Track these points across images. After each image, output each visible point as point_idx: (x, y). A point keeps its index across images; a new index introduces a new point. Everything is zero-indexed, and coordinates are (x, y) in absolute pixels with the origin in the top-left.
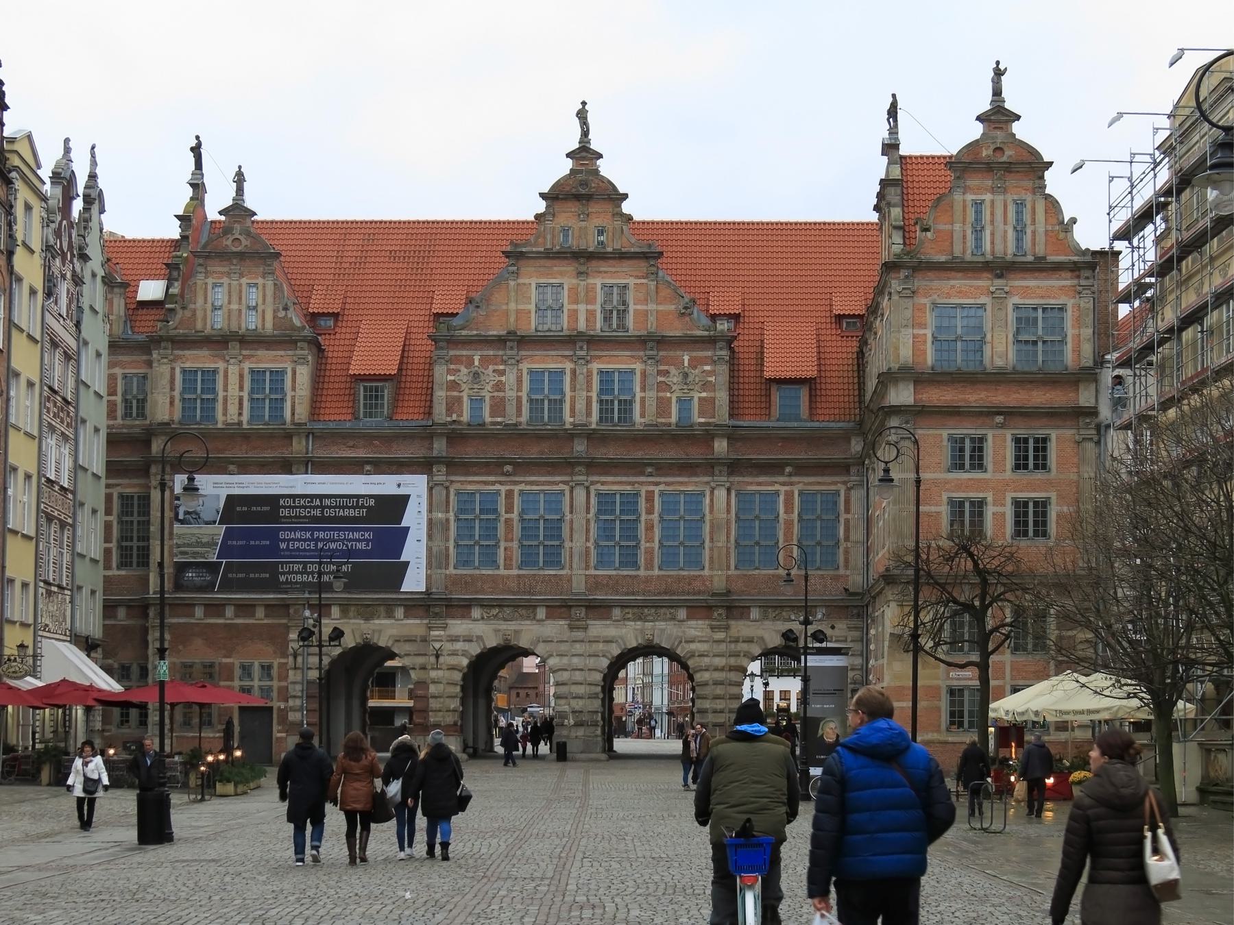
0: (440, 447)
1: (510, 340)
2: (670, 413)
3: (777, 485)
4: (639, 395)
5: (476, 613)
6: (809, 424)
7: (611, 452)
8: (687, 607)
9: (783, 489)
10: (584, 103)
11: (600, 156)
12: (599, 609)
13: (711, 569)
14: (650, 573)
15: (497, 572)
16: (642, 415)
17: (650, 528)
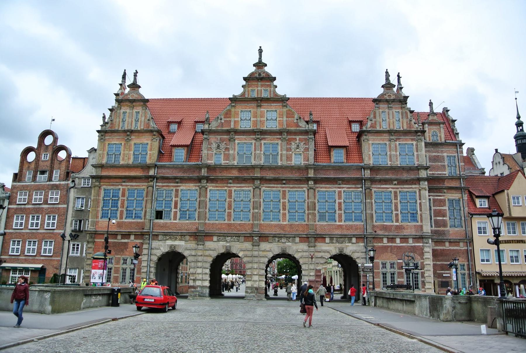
0: (204, 172)
1: (232, 132)
3: (334, 189)
4: (280, 153)
5: (215, 238)
6: (347, 164)
7: (270, 175)
8: (300, 237)
10: (260, 47)
11: (266, 65)
12: (264, 238)
13: (308, 221)
14: (285, 223)
15: (224, 222)
16: (281, 160)
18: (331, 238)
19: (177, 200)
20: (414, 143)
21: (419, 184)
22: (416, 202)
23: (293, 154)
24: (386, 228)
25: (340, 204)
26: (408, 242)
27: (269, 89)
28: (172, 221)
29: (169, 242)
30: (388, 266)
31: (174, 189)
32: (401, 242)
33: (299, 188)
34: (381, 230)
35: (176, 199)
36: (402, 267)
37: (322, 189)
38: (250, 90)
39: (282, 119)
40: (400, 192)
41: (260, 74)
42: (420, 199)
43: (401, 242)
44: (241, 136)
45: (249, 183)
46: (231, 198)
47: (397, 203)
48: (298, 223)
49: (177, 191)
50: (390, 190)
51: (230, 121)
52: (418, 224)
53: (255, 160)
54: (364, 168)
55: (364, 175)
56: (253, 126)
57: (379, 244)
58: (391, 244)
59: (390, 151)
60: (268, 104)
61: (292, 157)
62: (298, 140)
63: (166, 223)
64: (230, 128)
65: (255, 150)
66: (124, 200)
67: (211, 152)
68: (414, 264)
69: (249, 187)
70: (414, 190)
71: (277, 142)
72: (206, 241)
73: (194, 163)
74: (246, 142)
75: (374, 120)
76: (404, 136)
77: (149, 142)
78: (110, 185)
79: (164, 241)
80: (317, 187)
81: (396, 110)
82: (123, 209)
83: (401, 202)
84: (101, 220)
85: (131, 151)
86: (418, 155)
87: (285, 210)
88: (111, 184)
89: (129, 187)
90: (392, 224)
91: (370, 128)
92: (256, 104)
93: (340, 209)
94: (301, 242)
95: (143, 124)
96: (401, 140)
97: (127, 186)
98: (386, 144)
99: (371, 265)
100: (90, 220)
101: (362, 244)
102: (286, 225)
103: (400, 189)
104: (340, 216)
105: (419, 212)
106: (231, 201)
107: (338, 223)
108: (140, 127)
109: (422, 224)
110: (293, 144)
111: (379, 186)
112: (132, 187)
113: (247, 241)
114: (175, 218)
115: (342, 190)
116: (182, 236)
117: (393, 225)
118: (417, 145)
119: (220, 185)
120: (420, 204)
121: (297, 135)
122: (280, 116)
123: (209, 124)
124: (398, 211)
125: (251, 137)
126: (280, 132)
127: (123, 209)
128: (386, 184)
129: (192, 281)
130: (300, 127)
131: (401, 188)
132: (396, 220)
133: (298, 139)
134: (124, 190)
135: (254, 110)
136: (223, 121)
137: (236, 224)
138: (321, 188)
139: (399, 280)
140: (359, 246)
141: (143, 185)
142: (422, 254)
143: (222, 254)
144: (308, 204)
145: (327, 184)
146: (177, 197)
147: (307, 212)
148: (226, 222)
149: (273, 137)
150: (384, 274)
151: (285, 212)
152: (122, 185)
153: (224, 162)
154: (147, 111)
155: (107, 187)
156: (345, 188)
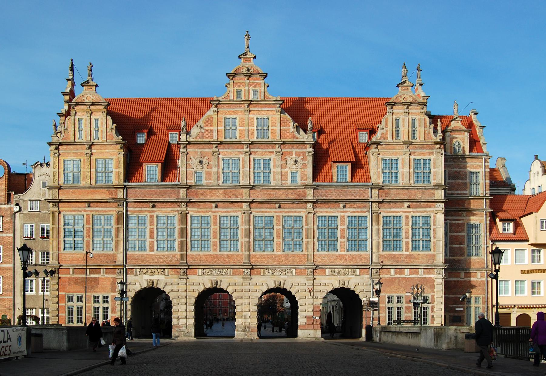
2: (287, 178)
4: (273, 170)
5: (199, 271)
9: (339, 214)
14: (279, 253)
17: (278, 233)
18: (333, 271)
19: (153, 228)
20: (432, 157)
21: (435, 207)
22: (430, 228)
23: (289, 172)
24: (394, 257)
25: (342, 230)
26: (417, 274)
27: (258, 89)
28: (148, 252)
29: (147, 277)
30: (395, 300)
31: (149, 215)
32: (411, 273)
33: (296, 212)
34: (389, 260)
35: (152, 227)
36: (410, 300)
37: (322, 214)
38: (235, 91)
39: (275, 128)
40: (412, 217)
41: (248, 70)
42: (434, 225)
43: (411, 273)
44: (226, 149)
45: (237, 207)
46: (216, 225)
47: (408, 229)
48: (294, 253)
49: (152, 217)
50: (401, 213)
51: (212, 131)
52: (430, 253)
53: (242, 180)
54: (371, 188)
55: (371, 197)
56: (240, 137)
57: (386, 276)
58: (398, 276)
59: (403, 167)
60: (258, 109)
61: (287, 176)
62: (294, 154)
63: (142, 255)
64: (212, 140)
65: (243, 167)
66: (90, 228)
67: (190, 170)
68: (424, 297)
69: (236, 211)
70: (429, 214)
71: (268, 157)
72: (189, 275)
73: (170, 183)
74: (232, 156)
75: (385, 129)
76: (420, 148)
77: (115, 158)
78: (71, 211)
79: (139, 276)
80: (317, 212)
81: (413, 117)
82: (89, 239)
83: (412, 229)
84: (64, 252)
85: (93, 169)
86: (435, 172)
87: (279, 239)
88: (71, 209)
89: (94, 213)
90: (401, 253)
91: (380, 138)
92: (244, 109)
93: (342, 237)
94: (298, 275)
95: (104, 135)
96: (416, 154)
97: (91, 211)
98: (398, 159)
99: (377, 299)
100: (51, 252)
101: (366, 276)
102: (281, 255)
103: (412, 214)
104: (342, 244)
105: (432, 240)
106: (216, 229)
107: (339, 253)
108: (102, 138)
109: (435, 253)
110: (289, 159)
111: (389, 210)
112: (98, 213)
113: (236, 275)
114: (152, 250)
115: (346, 214)
116: (161, 269)
117: (402, 255)
118: (434, 160)
119: (203, 210)
120: (434, 230)
121: (294, 148)
122: (273, 124)
123: (187, 135)
124: (409, 238)
125: (239, 150)
126: (272, 144)
127: (89, 239)
128: (396, 207)
129: (176, 320)
130: (297, 138)
131: (414, 212)
132: (406, 248)
133: (294, 153)
134: (88, 216)
135: (241, 116)
136: (203, 131)
137: (223, 255)
138: (321, 212)
139: (406, 315)
140: (363, 278)
141: (111, 211)
142: (433, 287)
143: (209, 289)
144: (306, 231)
145: (329, 208)
146: (153, 224)
147: (304, 240)
148: (211, 253)
149: (264, 150)
150: (390, 309)
151: (279, 240)
152: (85, 211)
153: (206, 182)
154: (109, 117)
155: (67, 213)
156: (350, 211)
